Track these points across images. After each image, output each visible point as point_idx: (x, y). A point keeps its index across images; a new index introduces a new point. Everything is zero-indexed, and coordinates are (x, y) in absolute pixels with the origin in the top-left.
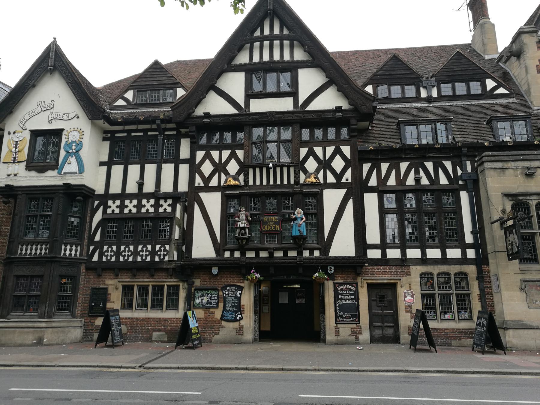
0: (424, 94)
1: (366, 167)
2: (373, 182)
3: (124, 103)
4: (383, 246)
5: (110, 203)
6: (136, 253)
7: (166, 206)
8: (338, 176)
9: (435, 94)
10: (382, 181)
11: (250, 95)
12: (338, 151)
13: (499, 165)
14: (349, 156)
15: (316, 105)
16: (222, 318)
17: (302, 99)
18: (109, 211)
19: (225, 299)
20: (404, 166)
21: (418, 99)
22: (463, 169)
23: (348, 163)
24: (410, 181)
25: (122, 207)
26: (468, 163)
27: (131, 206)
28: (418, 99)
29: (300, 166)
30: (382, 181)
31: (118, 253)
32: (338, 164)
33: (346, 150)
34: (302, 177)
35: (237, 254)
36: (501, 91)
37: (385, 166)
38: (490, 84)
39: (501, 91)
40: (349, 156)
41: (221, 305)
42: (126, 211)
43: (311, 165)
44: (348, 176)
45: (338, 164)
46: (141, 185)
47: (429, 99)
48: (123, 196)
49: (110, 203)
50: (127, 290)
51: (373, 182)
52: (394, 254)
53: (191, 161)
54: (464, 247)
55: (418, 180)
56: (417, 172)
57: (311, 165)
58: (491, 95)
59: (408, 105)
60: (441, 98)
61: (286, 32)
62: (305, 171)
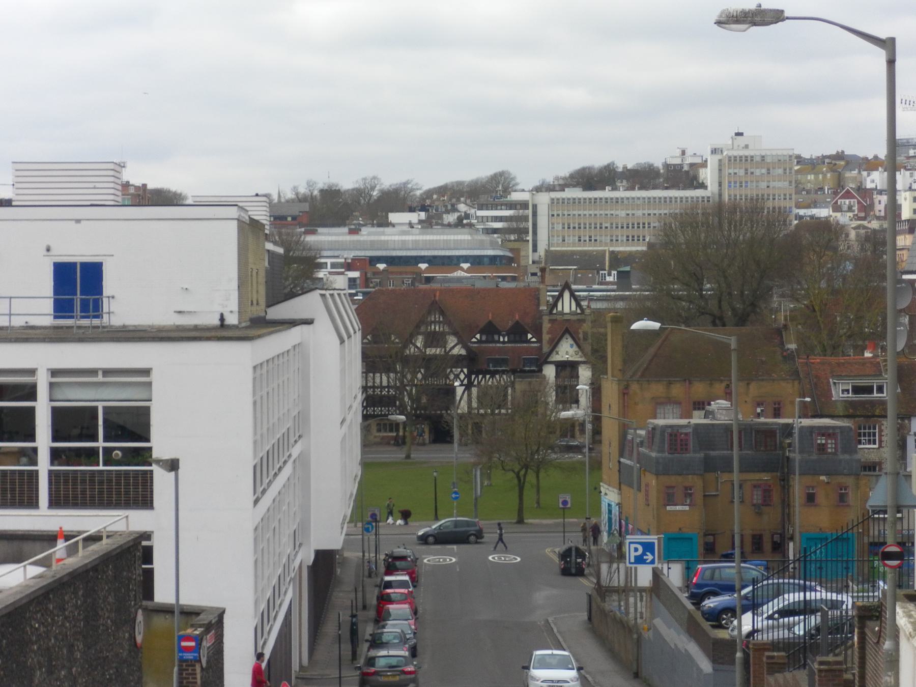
0: (501, 339)
1: (473, 376)
2: (476, 383)
3: (367, 341)
4: (478, 408)
5: (369, 390)
6: (381, 411)
7: (392, 392)
8: (462, 381)
9: (506, 339)
10: (479, 383)
11: (426, 346)
12: (462, 371)
13: (520, 380)
14: (466, 373)
15: (456, 351)
16: (417, 435)
17: (448, 349)
18: (368, 393)
19: (418, 429)
20: (488, 376)
21: (499, 342)
22: (510, 378)
23: (466, 376)
24: (490, 383)
25: (374, 391)
26: (512, 376)
27: (378, 391)
28: (499, 342)
29: (447, 377)
30: (479, 383)
31: (374, 411)
32: (462, 376)
33: (465, 370)
34: (448, 381)
35: (423, 412)
36: (534, 340)
37: (480, 377)
38: (530, 336)
39: (534, 340)
40: (466, 373)
41: (417, 431)
42: (376, 393)
43: (452, 376)
44: (466, 382)
45: (462, 376)
46: (381, 382)
47: (504, 342)
48: (374, 387)
49: (369, 390)
50: (378, 425)
51: (476, 383)
52: (482, 411)
53: (402, 372)
54: (507, 409)
55: (492, 382)
56: (493, 379)
57: (452, 376)
58: (529, 341)
59: (494, 345)
60: (509, 342)
61: (441, 319)
62: (449, 379)
